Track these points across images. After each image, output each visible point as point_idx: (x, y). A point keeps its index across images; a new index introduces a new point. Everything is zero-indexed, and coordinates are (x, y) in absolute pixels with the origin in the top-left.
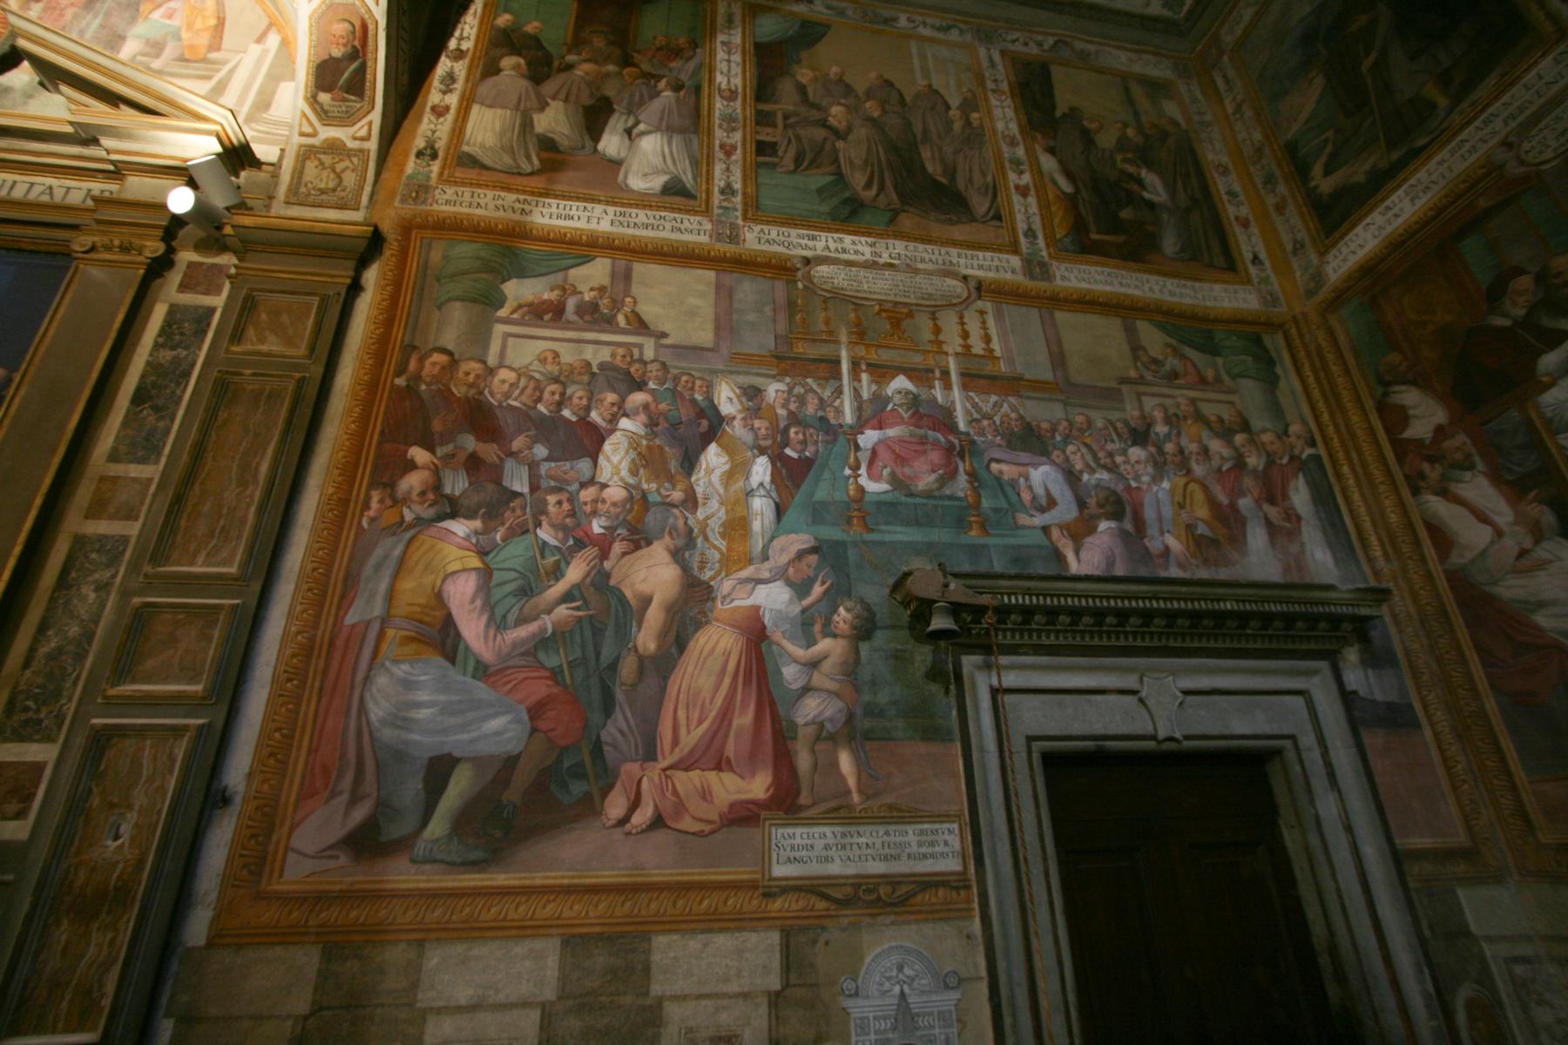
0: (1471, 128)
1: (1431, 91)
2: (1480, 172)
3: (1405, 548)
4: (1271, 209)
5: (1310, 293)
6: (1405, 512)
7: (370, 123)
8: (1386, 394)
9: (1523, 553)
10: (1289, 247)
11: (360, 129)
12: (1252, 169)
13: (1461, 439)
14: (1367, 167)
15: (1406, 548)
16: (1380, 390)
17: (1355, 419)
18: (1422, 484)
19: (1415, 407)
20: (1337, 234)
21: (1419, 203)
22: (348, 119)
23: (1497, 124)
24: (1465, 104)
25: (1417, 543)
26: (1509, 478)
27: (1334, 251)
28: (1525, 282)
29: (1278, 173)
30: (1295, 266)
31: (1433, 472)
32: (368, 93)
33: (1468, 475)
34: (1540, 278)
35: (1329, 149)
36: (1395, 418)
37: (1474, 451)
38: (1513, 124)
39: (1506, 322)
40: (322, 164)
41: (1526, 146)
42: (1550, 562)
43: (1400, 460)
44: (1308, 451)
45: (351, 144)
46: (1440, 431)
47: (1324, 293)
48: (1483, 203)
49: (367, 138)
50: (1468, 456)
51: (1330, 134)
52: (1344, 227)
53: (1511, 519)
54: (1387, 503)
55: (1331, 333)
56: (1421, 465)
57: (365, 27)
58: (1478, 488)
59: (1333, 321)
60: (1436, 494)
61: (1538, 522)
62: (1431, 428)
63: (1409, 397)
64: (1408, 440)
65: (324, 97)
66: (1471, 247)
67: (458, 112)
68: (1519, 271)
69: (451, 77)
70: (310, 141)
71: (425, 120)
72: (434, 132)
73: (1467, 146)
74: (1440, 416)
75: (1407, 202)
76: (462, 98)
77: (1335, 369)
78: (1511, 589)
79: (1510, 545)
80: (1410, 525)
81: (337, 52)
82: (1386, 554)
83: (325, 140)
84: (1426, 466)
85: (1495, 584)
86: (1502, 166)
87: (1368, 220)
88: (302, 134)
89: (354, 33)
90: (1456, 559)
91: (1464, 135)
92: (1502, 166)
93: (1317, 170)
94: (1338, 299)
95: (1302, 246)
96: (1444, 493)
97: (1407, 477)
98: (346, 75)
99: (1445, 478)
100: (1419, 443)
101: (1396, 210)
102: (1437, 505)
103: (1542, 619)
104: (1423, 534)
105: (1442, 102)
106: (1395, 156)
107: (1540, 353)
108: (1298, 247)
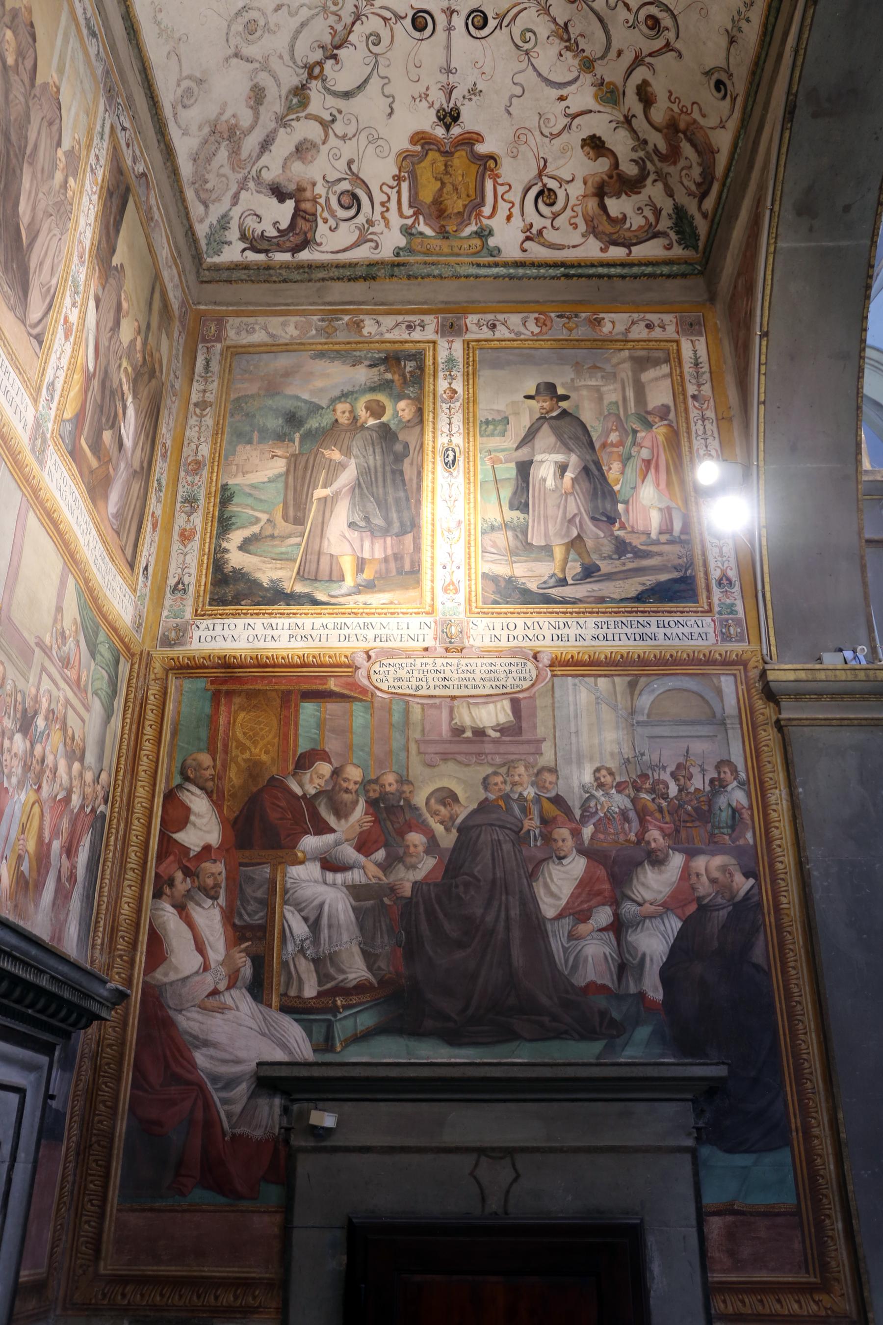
0: (356, 620)
1: (347, 565)
2: (343, 659)
3: (121, 945)
4: (176, 529)
5: (167, 642)
6: (139, 911)
8: (180, 787)
9: (215, 993)
10: (172, 581)
12: (182, 474)
13: (219, 867)
14: (276, 575)
15: (121, 945)
16: (177, 780)
17: (141, 792)
18: (167, 890)
19: (198, 815)
20: (220, 609)
21: (294, 644)
23: (370, 634)
24: (361, 598)
25: (134, 945)
26: (237, 921)
27: (210, 622)
28: (324, 769)
29: (202, 503)
30: (167, 603)
31: (182, 884)
33: (209, 902)
34: (336, 773)
35: (256, 529)
36: (176, 815)
37: (223, 885)
38: (378, 644)
39: (298, 791)
41: (376, 667)
42: (230, 1009)
43: (161, 856)
44: (102, 808)
46: (207, 848)
47: (178, 652)
48: (333, 685)
50: (217, 886)
51: (264, 517)
52: (230, 609)
53: (221, 958)
54: (128, 892)
55: (165, 692)
56: (172, 869)
58: (209, 919)
59: (173, 684)
60: (173, 906)
61: (238, 971)
62: (202, 844)
63: (198, 803)
64: (175, 841)
66: (308, 710)
68: (324, 756)
73: (346, 632)
74: (214, 838)
75: (285, 634)
77: (149, 732)
78: (190, 1021)
79: (209, 981)
80: (137, 925)
82: (102, 944)
84: (179, 875)
85: (180, 1011)
86: (357, 668)
87: (251, 621)
90: (159, 975)
91: (349, 621)
92: (357, 668)
93: (236, 537)
94: (188, 668)
95: (185, 591)
96: (181, 908)
97: (157, 875)
99: (188, 895)
100: (186, 850)
101: (275, 633)
102: (169, 916)
103: (200, 1058)
104: (144, 938)
105: (349, 581)
106: (300, 588)
107: (307, 832)
108: (179, 588)
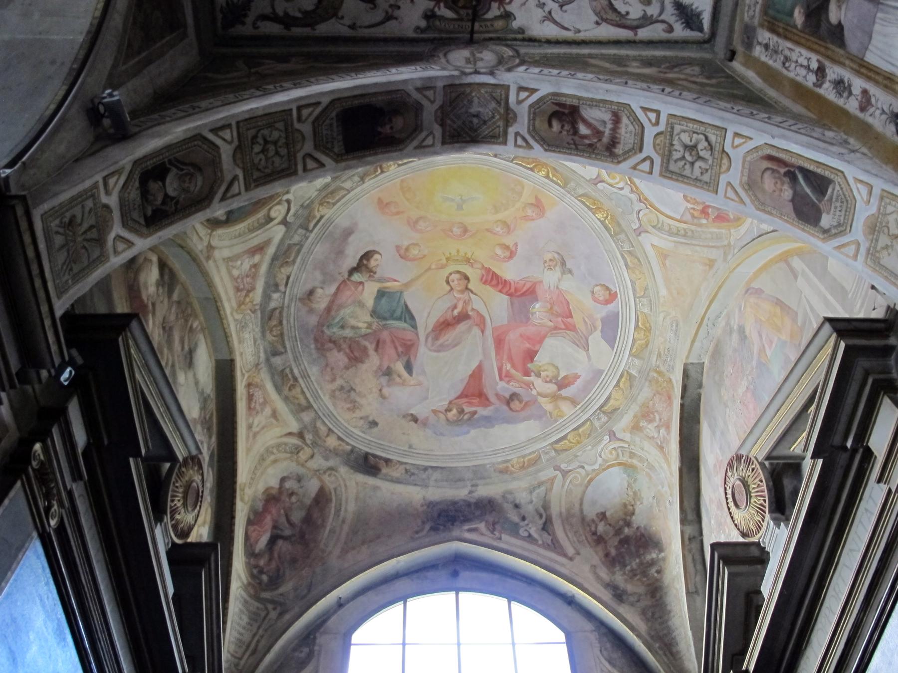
7: (857, 180)
11: (860, 193)
22: (848, 204)
32: (827, 174)
40: (886, 247)
45: (873, 209)
49: (871, 188)
57: (770, 158)
65: (826, 221)
67: (869, 78)
69: (840, 85)
70: (863, 250)
71: (870, 120)
72: (883, 112)
76: (858, 73)
81: (788, 193)
83: (865, 235)
88: (855, 257)
89: (773, 171)
98: (808, 191)
